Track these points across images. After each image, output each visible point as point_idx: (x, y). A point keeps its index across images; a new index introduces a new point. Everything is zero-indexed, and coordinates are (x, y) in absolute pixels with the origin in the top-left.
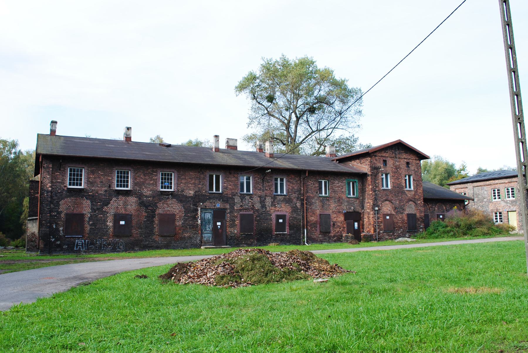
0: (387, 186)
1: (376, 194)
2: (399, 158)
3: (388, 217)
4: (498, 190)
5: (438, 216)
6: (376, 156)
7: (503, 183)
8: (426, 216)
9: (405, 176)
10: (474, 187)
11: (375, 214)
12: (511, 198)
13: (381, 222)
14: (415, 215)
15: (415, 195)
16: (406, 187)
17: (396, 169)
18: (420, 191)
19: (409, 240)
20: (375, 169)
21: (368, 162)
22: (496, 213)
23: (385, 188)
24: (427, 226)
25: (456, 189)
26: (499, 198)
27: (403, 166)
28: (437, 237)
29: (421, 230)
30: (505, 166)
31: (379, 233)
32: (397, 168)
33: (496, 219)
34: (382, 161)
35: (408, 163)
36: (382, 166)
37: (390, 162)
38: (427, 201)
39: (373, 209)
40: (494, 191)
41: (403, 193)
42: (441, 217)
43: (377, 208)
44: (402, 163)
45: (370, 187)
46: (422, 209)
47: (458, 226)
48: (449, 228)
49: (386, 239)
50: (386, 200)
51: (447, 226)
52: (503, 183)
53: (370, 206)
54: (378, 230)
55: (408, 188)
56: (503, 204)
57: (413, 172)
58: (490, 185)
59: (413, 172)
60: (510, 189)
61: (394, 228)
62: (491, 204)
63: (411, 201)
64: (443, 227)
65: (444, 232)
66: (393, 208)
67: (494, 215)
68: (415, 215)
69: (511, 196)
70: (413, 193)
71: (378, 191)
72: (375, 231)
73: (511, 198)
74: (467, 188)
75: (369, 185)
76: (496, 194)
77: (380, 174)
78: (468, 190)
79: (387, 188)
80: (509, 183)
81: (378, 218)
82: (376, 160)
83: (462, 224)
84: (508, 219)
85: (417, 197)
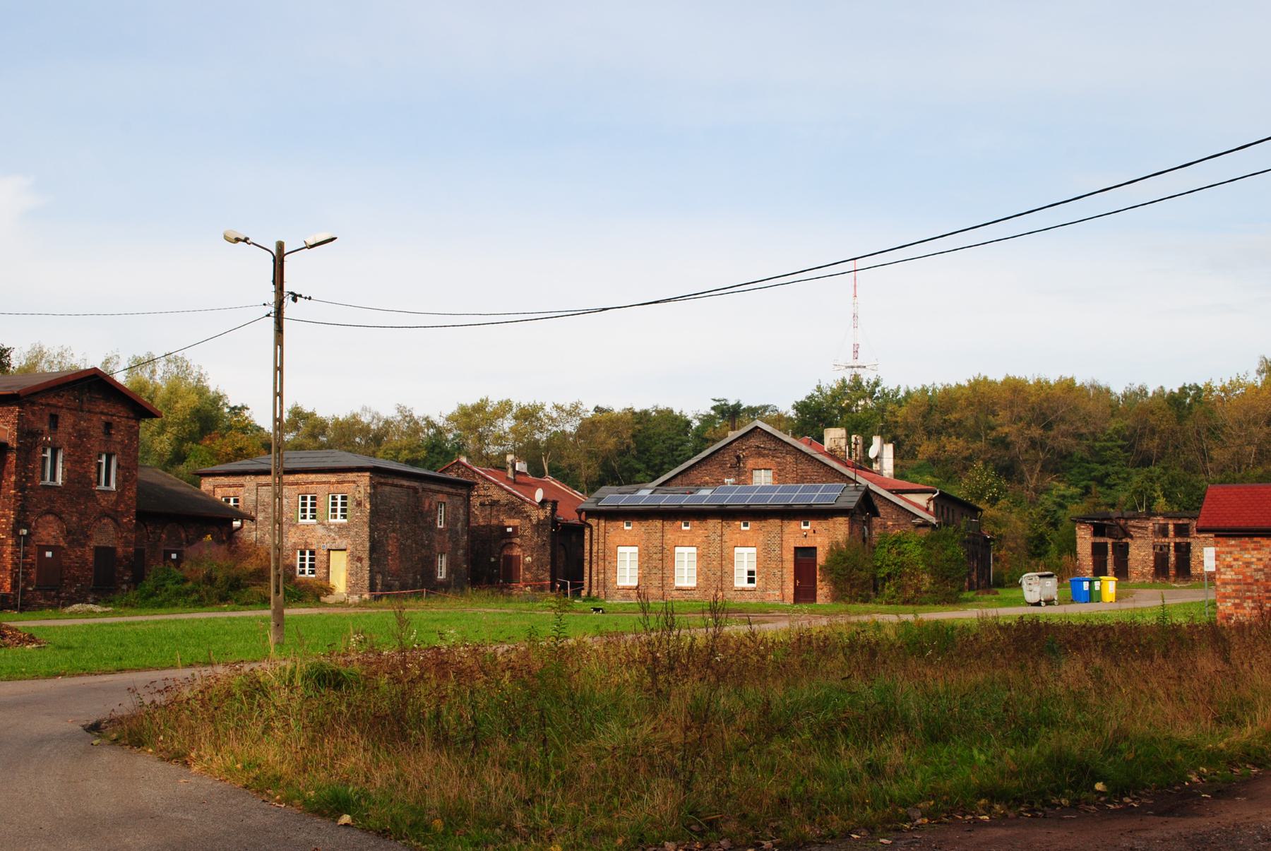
0: (53, 477)
1: (25, 498)
2: (89, 412)
3: (49, 554)
4: (313, 498)
5: (167, 555)
6: (33, 404)
7: (324, 483)
8: (139, 553)
9: (100, 457)
10: (258, 485)
11: (18, 545)
12: (340, 520)
13: (32, 565)
14: (113, 550)
15: (117, 503)
16: (98, 483)
17: (80, 437)
18: (131, 493)
19: (98, 609)
20: (28, 436)
21: (11, 418)
22: (303, 553)
23: (48, 481)
24: (138, 579)
25: (215, 487)
26: (314, 517)
27: (97, 432)
28: (160, 605)
29: (125, 587)
30: (365, 409)
31: (24, 591)
32: (82, 435)
33: (303, 566)
34: (46, 418)
35: (108, 426)
36: (46, 427)
37: (67, 421)
38: (145, 517)
39: (15, 532)
40: (304, 498)
41: (91, 495)
42: (174, 556)
43: (25, 532)
44: (95, 426)
45: (13, 478)
46: (132, 537)
47: (210, 580)
48: (189, 585)
49: (41, 607)
50: (49, 512)
51: (185, 580)
52: (324, 483)
53: (6, 524)
54: (21, 584)
55: (102, 486)
56: (320, 531)
57: (119, 447)
58: (297, 484)
59: (119, 447)
60: (339, 497)
61: (62, 580)
62: (293, 530)
63: (108, 516)
64: (177, 582)
65: (178, 594)
66: (62, 532)
67: (299, 556)
68: (113, 550)
69: (339, 513)
70: (114, 498)
71: (31, 488)
72: (14, 585)
73: (340, 520)
74: (242, 486)
75: (10, 474)
76: (309, 508)
77: (40, 449)
78: (243, 493)
79: (51, 484)
80: (338, 483)
81: (25, 556)
82: (34, 414)
83: (220, 575)
84: (328, 568)
85: (122, 507)
